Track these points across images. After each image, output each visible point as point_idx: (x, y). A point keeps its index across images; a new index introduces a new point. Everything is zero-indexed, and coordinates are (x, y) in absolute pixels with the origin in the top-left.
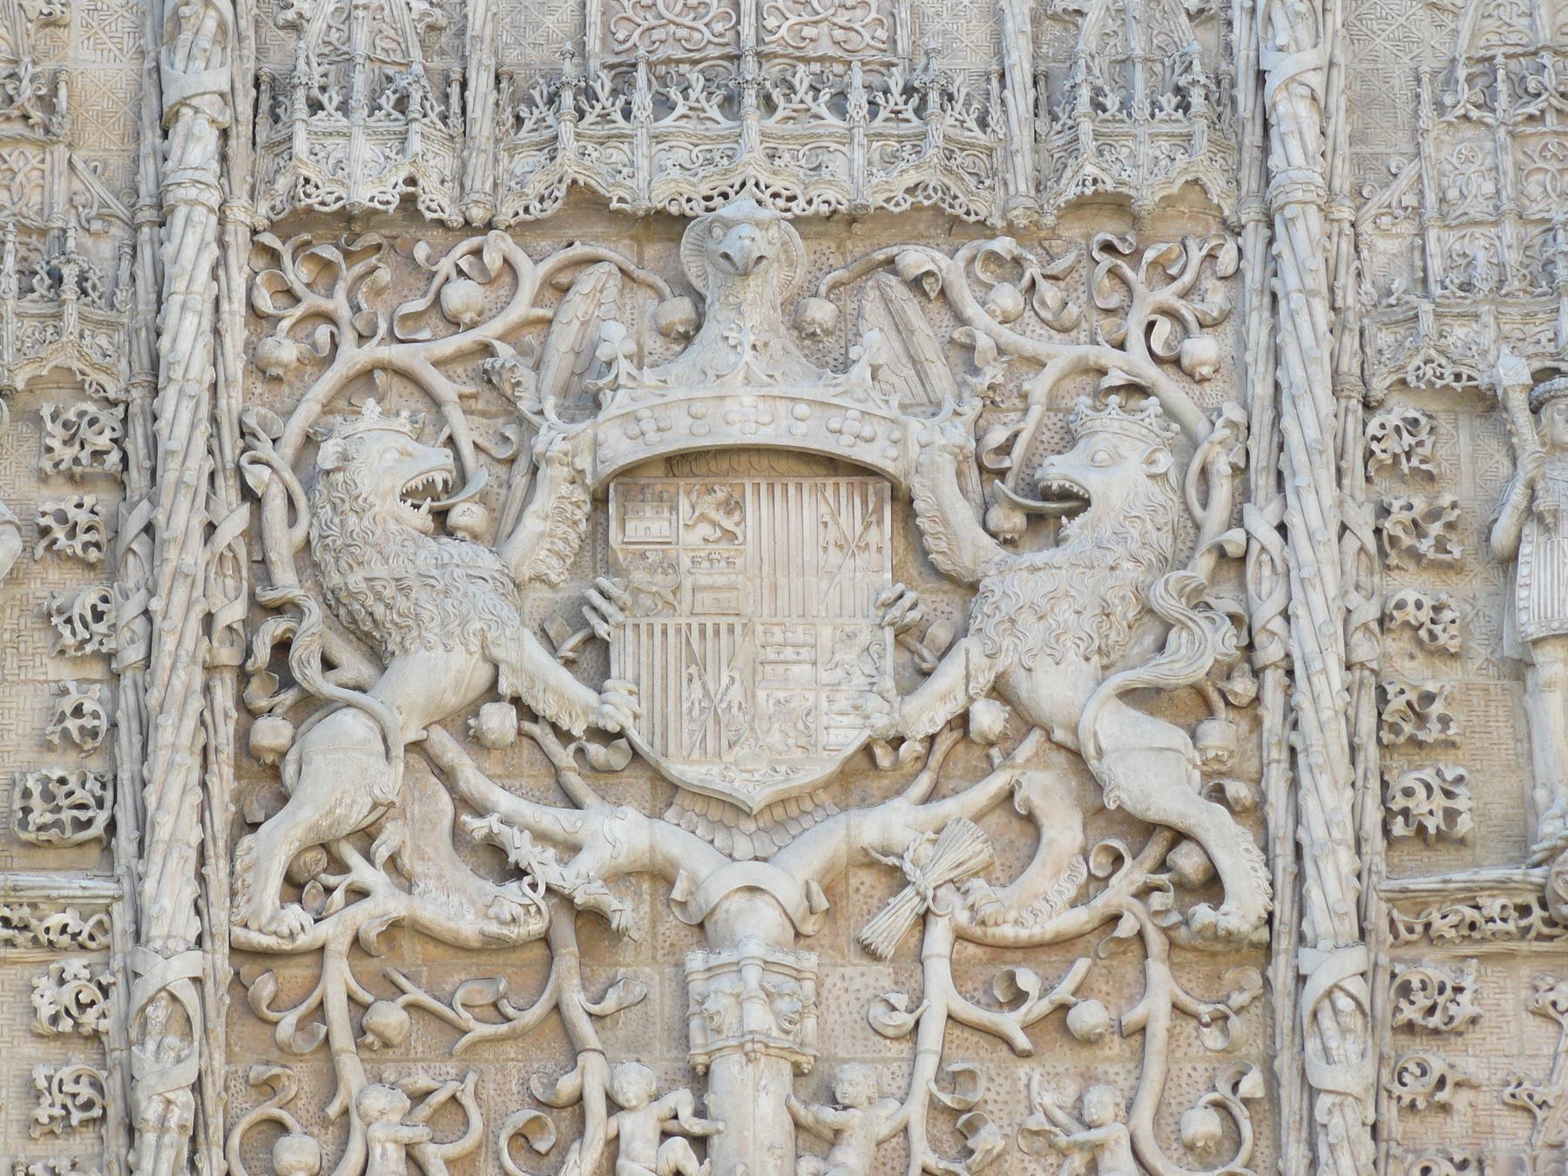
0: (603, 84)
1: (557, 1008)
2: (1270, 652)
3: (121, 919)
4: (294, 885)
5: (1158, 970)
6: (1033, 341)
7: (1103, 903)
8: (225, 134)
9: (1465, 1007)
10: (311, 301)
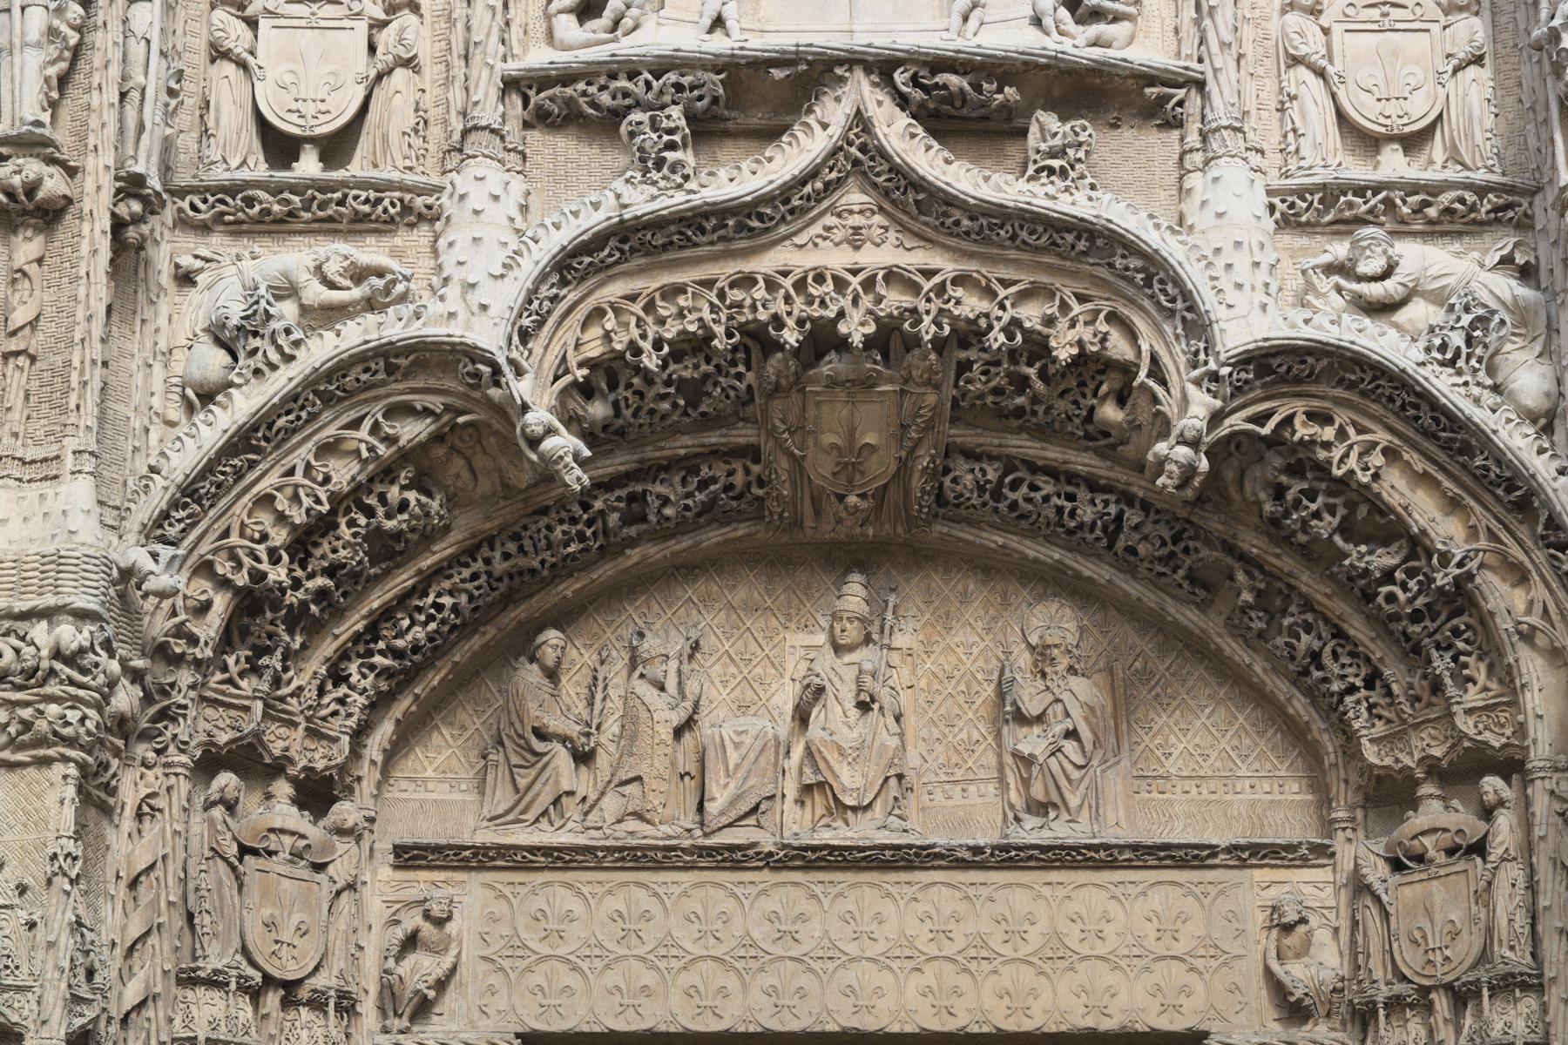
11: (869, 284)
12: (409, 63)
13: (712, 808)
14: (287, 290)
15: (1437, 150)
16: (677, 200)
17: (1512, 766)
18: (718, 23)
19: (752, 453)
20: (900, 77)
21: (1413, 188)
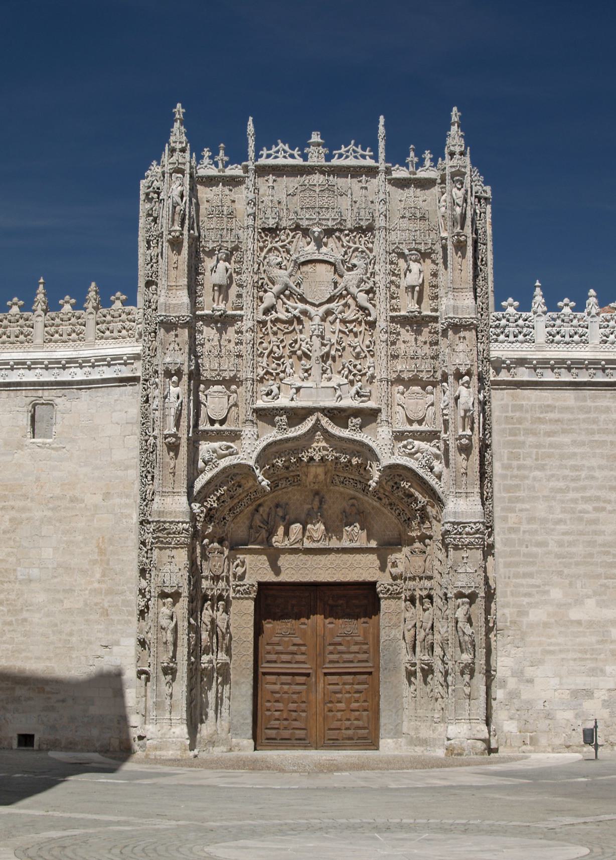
0: (300, 210)
1: (294, 329)
2: (377, 285)
3: (244, 318)
4: (264, 314)
5: (363, 324)
6: (351, 244)
7: (357, 316)
8: (255, 218)
9: (398, 330)
10: (265, 238)
11: (319, 450)
12: (236, 405)
13: (291, 541)
14: (214, 451)
15: (424, 423)
16: (286, 436)
17: (430, 538)
18: (292, 399)
19: (299, 476)
20: (326, 412)
21: (418, 431)
